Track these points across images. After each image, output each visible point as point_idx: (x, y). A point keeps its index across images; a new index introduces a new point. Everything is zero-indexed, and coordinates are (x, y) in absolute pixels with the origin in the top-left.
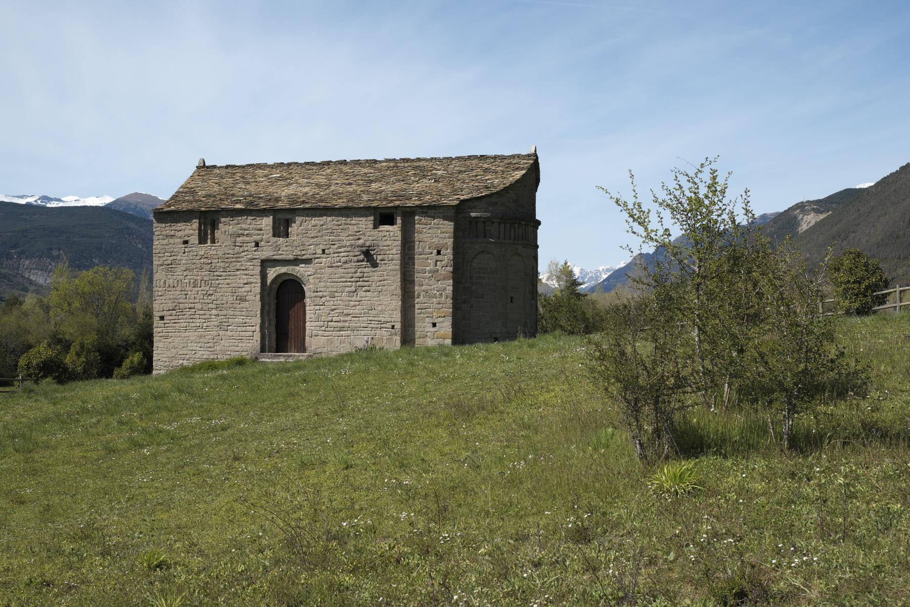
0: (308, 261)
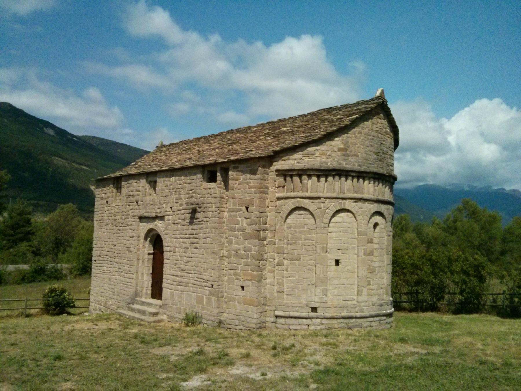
0: (162, 218)
